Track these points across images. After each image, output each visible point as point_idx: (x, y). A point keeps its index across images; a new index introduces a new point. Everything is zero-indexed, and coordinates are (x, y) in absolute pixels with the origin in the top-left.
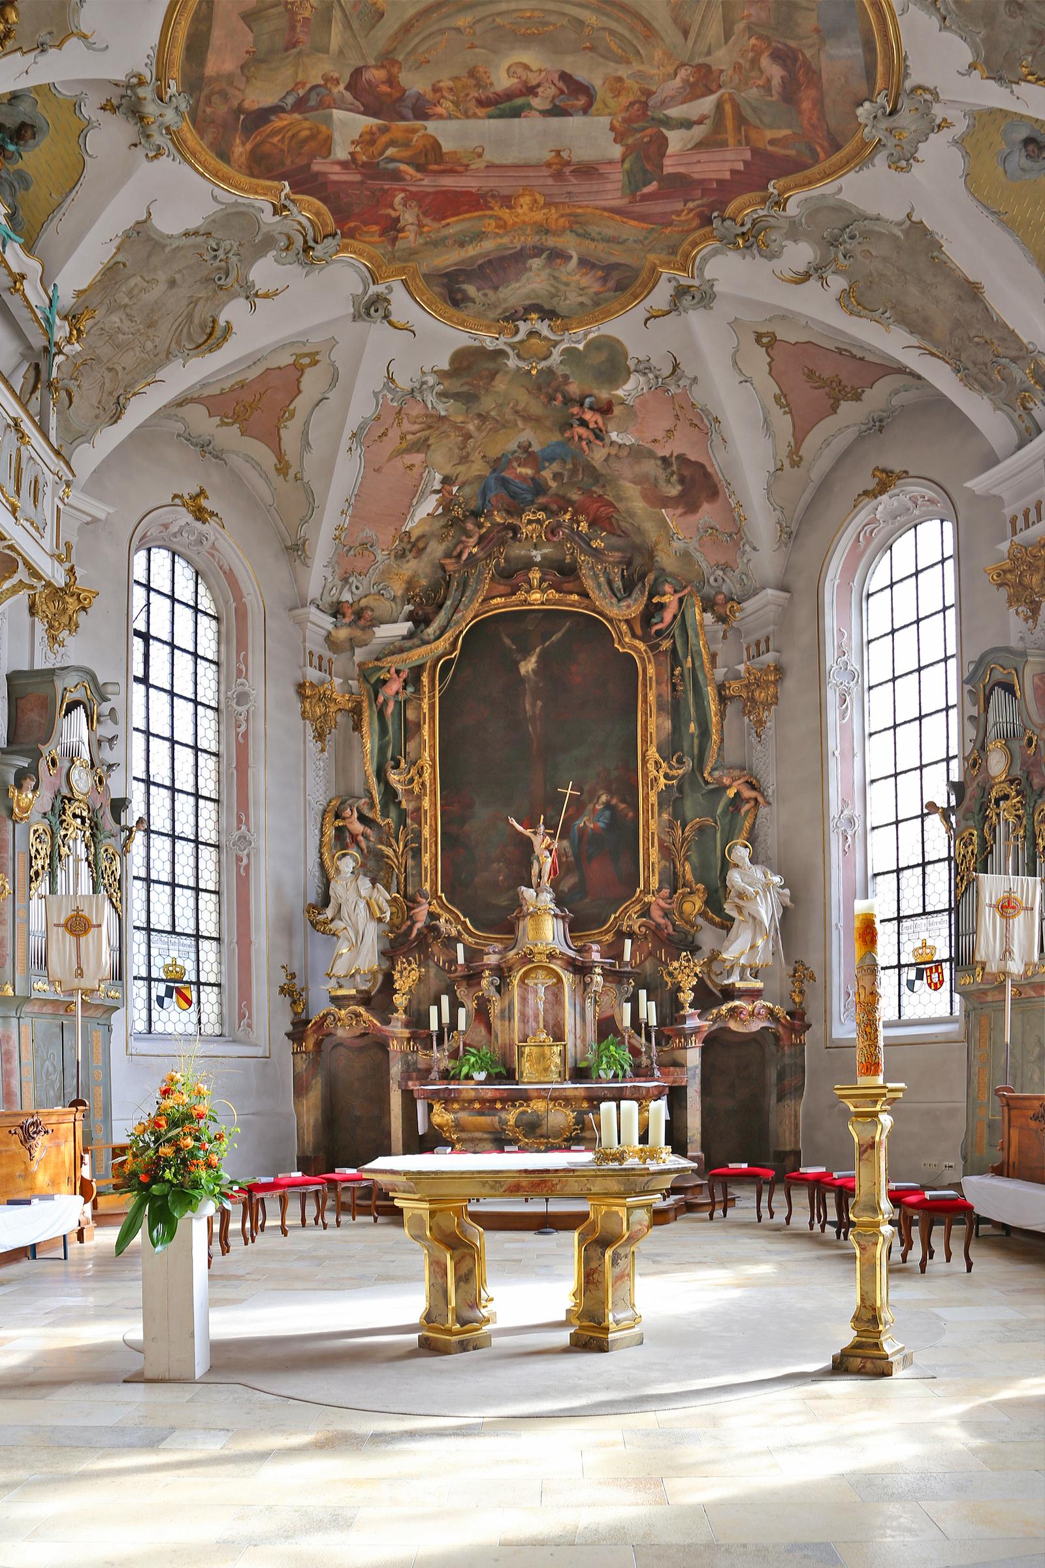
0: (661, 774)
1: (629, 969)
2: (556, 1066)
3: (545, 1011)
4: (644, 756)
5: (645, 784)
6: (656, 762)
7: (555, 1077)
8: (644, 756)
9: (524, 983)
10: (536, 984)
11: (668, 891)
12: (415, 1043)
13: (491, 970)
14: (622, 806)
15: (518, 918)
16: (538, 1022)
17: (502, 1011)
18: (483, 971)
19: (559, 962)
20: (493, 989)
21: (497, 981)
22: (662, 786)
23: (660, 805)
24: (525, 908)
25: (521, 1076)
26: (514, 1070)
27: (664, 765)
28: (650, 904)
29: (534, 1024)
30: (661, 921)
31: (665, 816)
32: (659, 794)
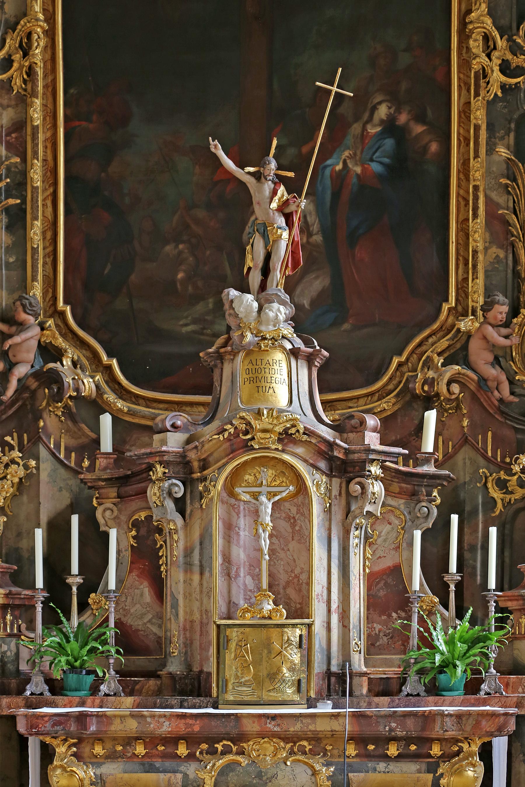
0: (496, 62)
1: (429, 469)
2: (291, 669)
3: (272, 551)
4: (463, 24)
5: (464, 85)
6: (486, 38)
7: (290, 691)
8: (463, 24)
9: (232, 494)
10: (256, 496)
11: (505, 309)
12: (15, 618)
13: (165, 464)
14: (419, 129)
15: (220, 357)
16: (257, 578)
17: (188, 553)
18: (150, 467)
19: (300, 450)
20: (170, 505)
21: (179, 491)
22: (495, 90)
23: (490, 127)
24: (235, 335)
25: (223, 686)
26: (209, 674)
27: (501, 43)
28: (469, 336)
29: (249, 580)
30: (492, 372)
31: (503, 152)
32: (490, 104)
